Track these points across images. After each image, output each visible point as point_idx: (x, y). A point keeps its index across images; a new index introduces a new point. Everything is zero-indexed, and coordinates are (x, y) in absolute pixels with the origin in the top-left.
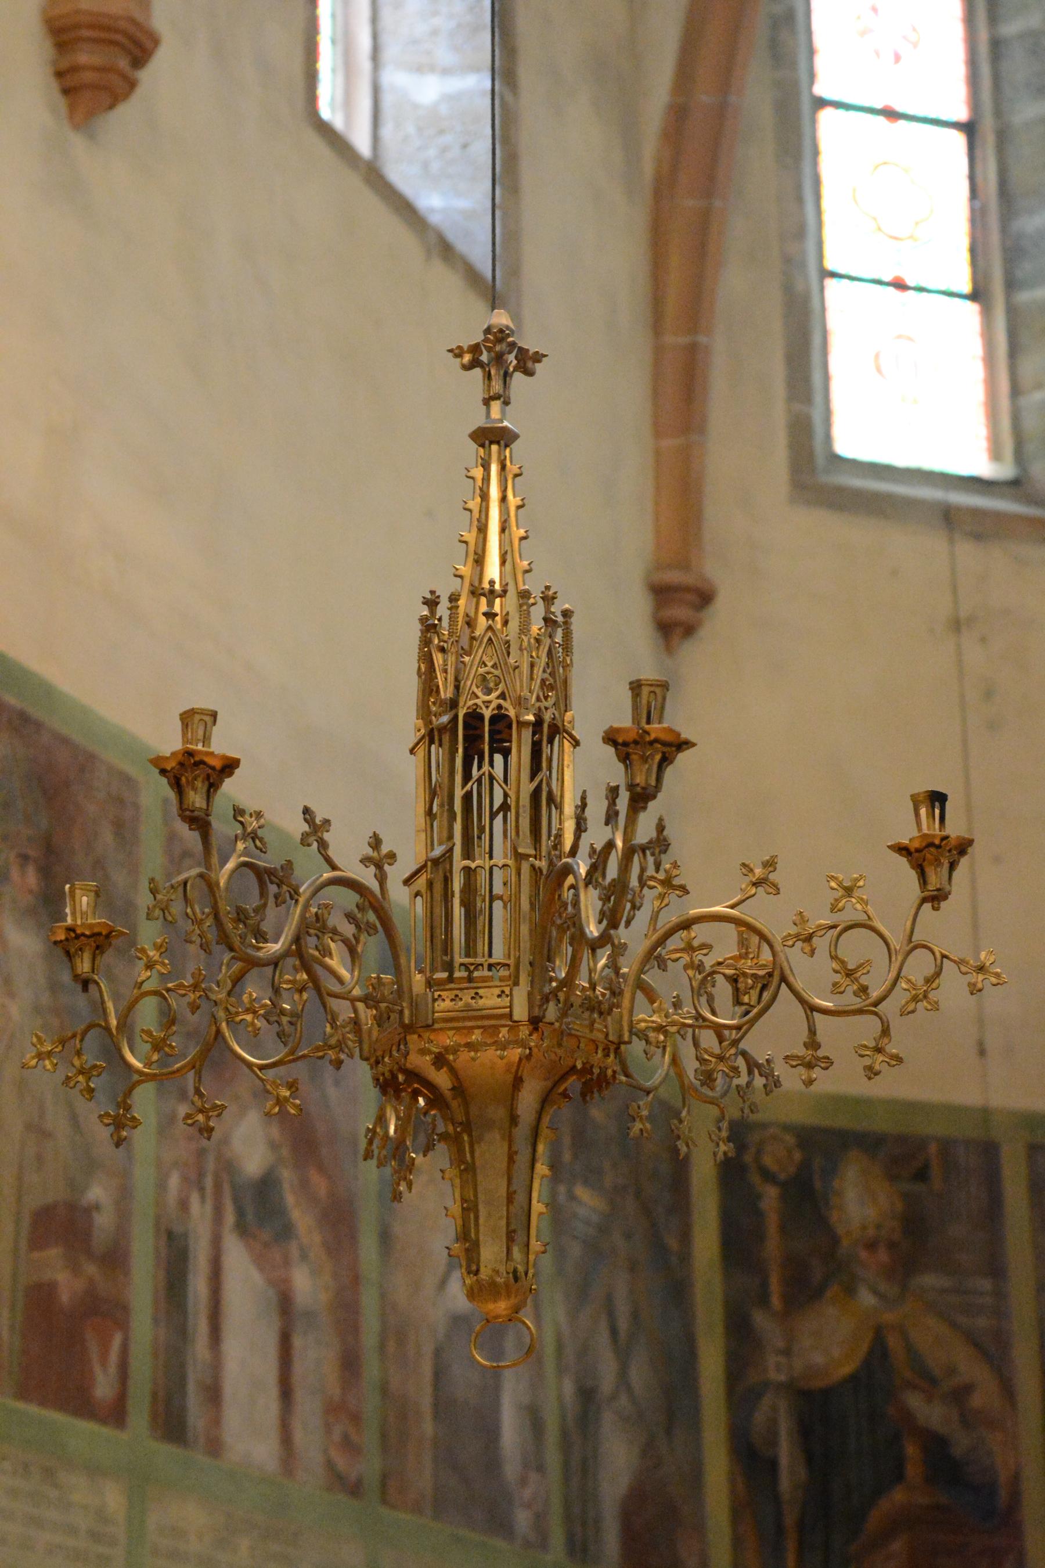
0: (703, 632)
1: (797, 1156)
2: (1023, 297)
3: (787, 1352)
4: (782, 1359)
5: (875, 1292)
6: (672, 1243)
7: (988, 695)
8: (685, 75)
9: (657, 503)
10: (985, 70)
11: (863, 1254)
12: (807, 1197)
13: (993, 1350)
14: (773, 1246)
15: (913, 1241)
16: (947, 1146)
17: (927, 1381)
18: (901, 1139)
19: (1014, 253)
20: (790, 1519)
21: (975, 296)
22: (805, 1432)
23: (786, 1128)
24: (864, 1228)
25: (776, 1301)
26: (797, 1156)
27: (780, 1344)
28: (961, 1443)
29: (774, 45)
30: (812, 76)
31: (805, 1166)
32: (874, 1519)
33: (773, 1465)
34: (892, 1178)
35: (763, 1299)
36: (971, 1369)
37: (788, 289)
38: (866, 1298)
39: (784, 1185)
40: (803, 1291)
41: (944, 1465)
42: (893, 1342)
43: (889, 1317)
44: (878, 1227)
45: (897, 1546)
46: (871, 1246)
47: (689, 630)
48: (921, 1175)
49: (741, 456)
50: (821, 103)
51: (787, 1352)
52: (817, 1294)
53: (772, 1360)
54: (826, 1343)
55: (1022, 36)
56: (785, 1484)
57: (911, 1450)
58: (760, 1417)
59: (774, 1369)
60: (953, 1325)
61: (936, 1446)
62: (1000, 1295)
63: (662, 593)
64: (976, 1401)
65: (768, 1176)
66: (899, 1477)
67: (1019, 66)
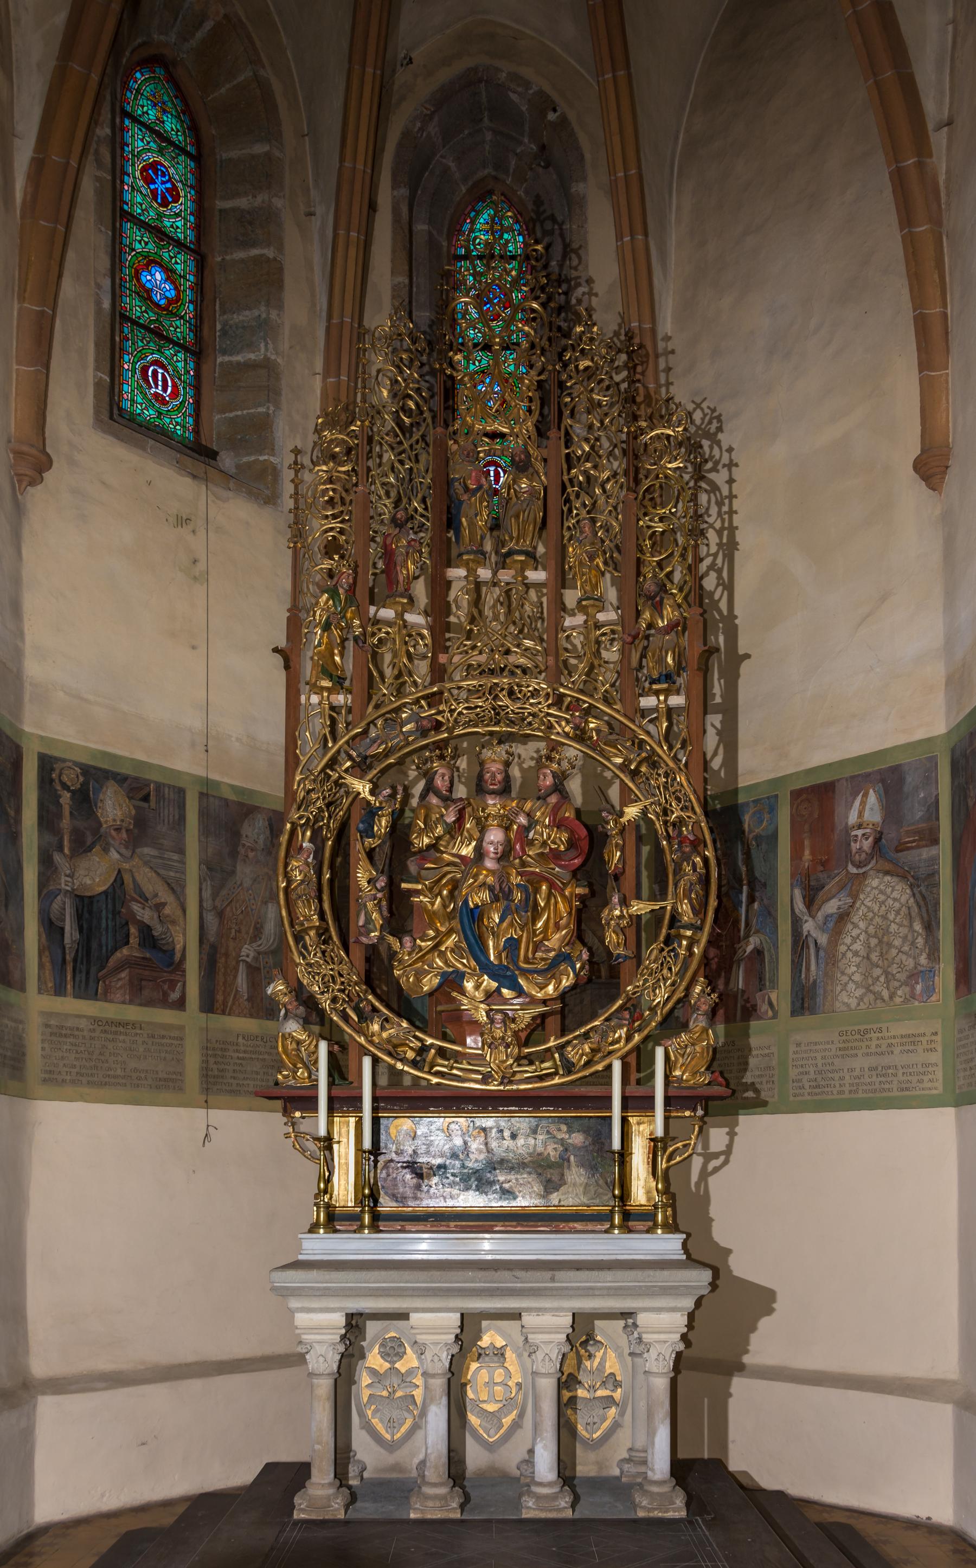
1: (81, 779)
3: (71, 876)
4: (69, 879)
5: (118, 852)
6: (12, 813)
12: (85, 800)
13: (176, 888)
14: (66, 823)
17: (143, 898)
18: (136, 779)
20: (69, 958)
22: (79, 917)
23: (76, 764)
25: (66, 851)
26: (81, 779)
27: (68, 872)
28: (158, 930)
31: (85, 785)
32: (112, 962)
33: (62, 930)
35: (60, 848)
36: (165, 896)
39: (73, 792)
40: (81, 847)
42: (127, 878)
43: (126, 866)
51: (71, 876)
52: (90, 849)
53: (63, 879)
54: (94, 873)
56: (67, 940)
57: (133, 930)
58: (56, 906)
59: (64, 883)
60: (158, 874)
62: (183, 862)
64: (167, 911)
65: (65, 787)
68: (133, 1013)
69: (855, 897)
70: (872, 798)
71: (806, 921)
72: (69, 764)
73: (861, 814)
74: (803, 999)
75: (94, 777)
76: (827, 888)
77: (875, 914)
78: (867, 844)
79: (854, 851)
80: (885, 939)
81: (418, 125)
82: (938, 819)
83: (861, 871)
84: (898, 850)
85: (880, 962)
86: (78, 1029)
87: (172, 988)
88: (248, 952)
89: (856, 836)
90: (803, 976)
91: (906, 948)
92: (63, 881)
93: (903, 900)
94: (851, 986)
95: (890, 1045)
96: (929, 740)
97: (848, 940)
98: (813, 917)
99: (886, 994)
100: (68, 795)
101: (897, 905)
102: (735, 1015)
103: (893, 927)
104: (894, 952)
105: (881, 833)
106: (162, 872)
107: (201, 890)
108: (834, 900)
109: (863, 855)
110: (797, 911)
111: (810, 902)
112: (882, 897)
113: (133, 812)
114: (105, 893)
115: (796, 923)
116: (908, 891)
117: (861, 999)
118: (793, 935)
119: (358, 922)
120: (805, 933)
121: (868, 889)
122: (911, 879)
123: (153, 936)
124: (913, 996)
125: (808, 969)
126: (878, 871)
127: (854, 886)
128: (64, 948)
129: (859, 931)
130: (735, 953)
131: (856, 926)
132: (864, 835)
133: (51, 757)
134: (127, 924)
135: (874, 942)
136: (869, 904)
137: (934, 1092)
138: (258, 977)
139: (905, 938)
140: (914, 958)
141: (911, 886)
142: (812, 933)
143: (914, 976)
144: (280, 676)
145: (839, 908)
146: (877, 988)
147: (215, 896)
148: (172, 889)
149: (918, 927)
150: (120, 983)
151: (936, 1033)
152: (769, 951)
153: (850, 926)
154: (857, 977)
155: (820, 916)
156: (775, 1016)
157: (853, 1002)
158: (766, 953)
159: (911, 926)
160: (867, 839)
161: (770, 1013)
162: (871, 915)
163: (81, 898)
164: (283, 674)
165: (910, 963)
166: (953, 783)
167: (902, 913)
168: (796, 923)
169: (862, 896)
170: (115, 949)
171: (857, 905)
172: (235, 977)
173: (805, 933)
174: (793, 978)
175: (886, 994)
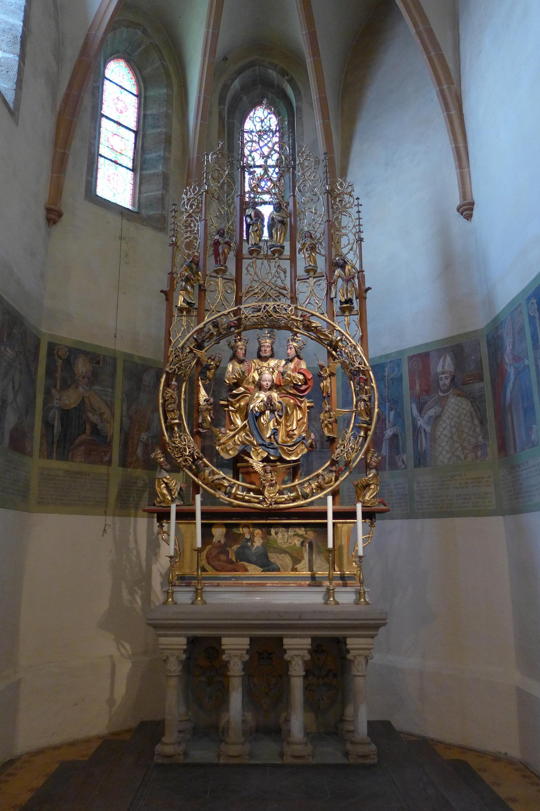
0: (59, 224)
1: (68, 353)
2: (145, 172)
3: (60, 400)
4: (58, 401)
5: (83, 388)
6: (33, 370)
7: (127, 256)
8: (70, 87)
9: (50, 188)
10: (142, 121)
11: (81, 379)
12: (69, 363)
13: (110, 405)
14: (58, 374)
15: (94, 378)
16: (105, 357)
19: (143, 162)
20: (55, 440)
21: (133, 170)
22: (62, 419)
23: (66, 346)
24: (82, 373)
25: (58, 388)
26: (68, 353)
27: (58, 398)
28: (100, 426)
29: (93, 94)
30: (101, 109)
31: (69, 356)
32: (77, 441)
33: (53, 426)
34: (90, 363)
35: (55, 387)
37: (90, 150)
38: (81, 389)
39: (63, 360)
40: (65, 386)
41: (95, 430)
42: (87, 400)
44: (86, 373)
45: (82, 448)
46: (84, 377)
47: (55, 222)
48: (98, 363)
49: (73, 185)
50: (103, 116)
51: (60, 400)
52: (69, 387)
53: (56, 401)
54: (70, 399)
55: (151, 115)
57: (88, 426)
58: (51, 414)
60: (102, 398)
61: (94, 427)
63: (49, 210)
64: (105, 416)
65: (60, 357)
66: (84, 432)
67: (150, 121)
68: (86, 467)
69: (443, 407)
70: (448, 359)
71: (419, 420)
72: (62, 346)
73: (443, 367)
74: (420, 459)
75: (75, 352)
76: (429, 403)
77: (454, 416)
78: (447, 382)
79: (441, 385)
80: (460, 428)
81: (230, 82)
82: (482, 369)
83: (446, 394)
84: (463, 384)
85: (458, 440)
86: (57, 476)
87: (106, 455)
88: (144, 436)
89: (442, 378)
90: (419, 447)
91: (471, 433)
92: (55, 402)
93: (468, 408)
94: (444, 452)
95: (466, 483)
96: (475, 331)
97: (441, 429)
98: (423, 418)
99: (462, 457)
100: (61, 361)
101: (465, 412)
102: (385, 467)
103: (464, 423)
104: (465, 435)
105: (454, 376)
106: (104, 398)
107: (122, 406)
108: (432, 409)
109: (446, 387)
110: (414, 415)
111: (420, 411)
112: (457, 408)
113: (92, 369)
114: (75, 408)
115: (414, 420)
116: (470, 404)
117: (449, 459)
118: (413, 427)
119: (198, 420)
120: (419, 426)
121: (450, 404)
122: (471, 399)
123: (97, 429)
124: (476, 457)
125: (421, 444)
126: (454, 395)
127: (442, 402)
128: (53, 435)
129: (446, 425)
130: (384, 436)
131: (444, 422)
132: (445, 377)
133: (54, 344)
134: (85, 423)
135: (454, 430)
136: (451, 411)
137: (491, 508)
138: (148, 449)
139: (470, 428)
140: (476, 438)
141: (471, 402)
142: (422, 426)
143: (476, 447)
144: (163, 305)
145: (435, 413)
146: (458, 453)
147: (129, 408)
148: (108, 406)
149: (476, 422)
150: (80, 453)
151: (490, 477)
152: (401, 434)
153: (441, 422)
154: (447, 448)
155: (426, 417)
156: (406, 468)
157: (446, 461)
158: (399, 436)
159: (473, 422)
160: (447, 379)
161: (403, 466)
162: (452, 416)
163: (63, 410)
164: (165, 303)
165: (473, 440)
166: (488, 351)
167: (468, 415)
168: (414, 420)
169: (446, 407)
170: (79, 435)
171: (445, 411)
172: (137, 449)
173: (419, 426)
174: (414, 448)
175: (462, 457)
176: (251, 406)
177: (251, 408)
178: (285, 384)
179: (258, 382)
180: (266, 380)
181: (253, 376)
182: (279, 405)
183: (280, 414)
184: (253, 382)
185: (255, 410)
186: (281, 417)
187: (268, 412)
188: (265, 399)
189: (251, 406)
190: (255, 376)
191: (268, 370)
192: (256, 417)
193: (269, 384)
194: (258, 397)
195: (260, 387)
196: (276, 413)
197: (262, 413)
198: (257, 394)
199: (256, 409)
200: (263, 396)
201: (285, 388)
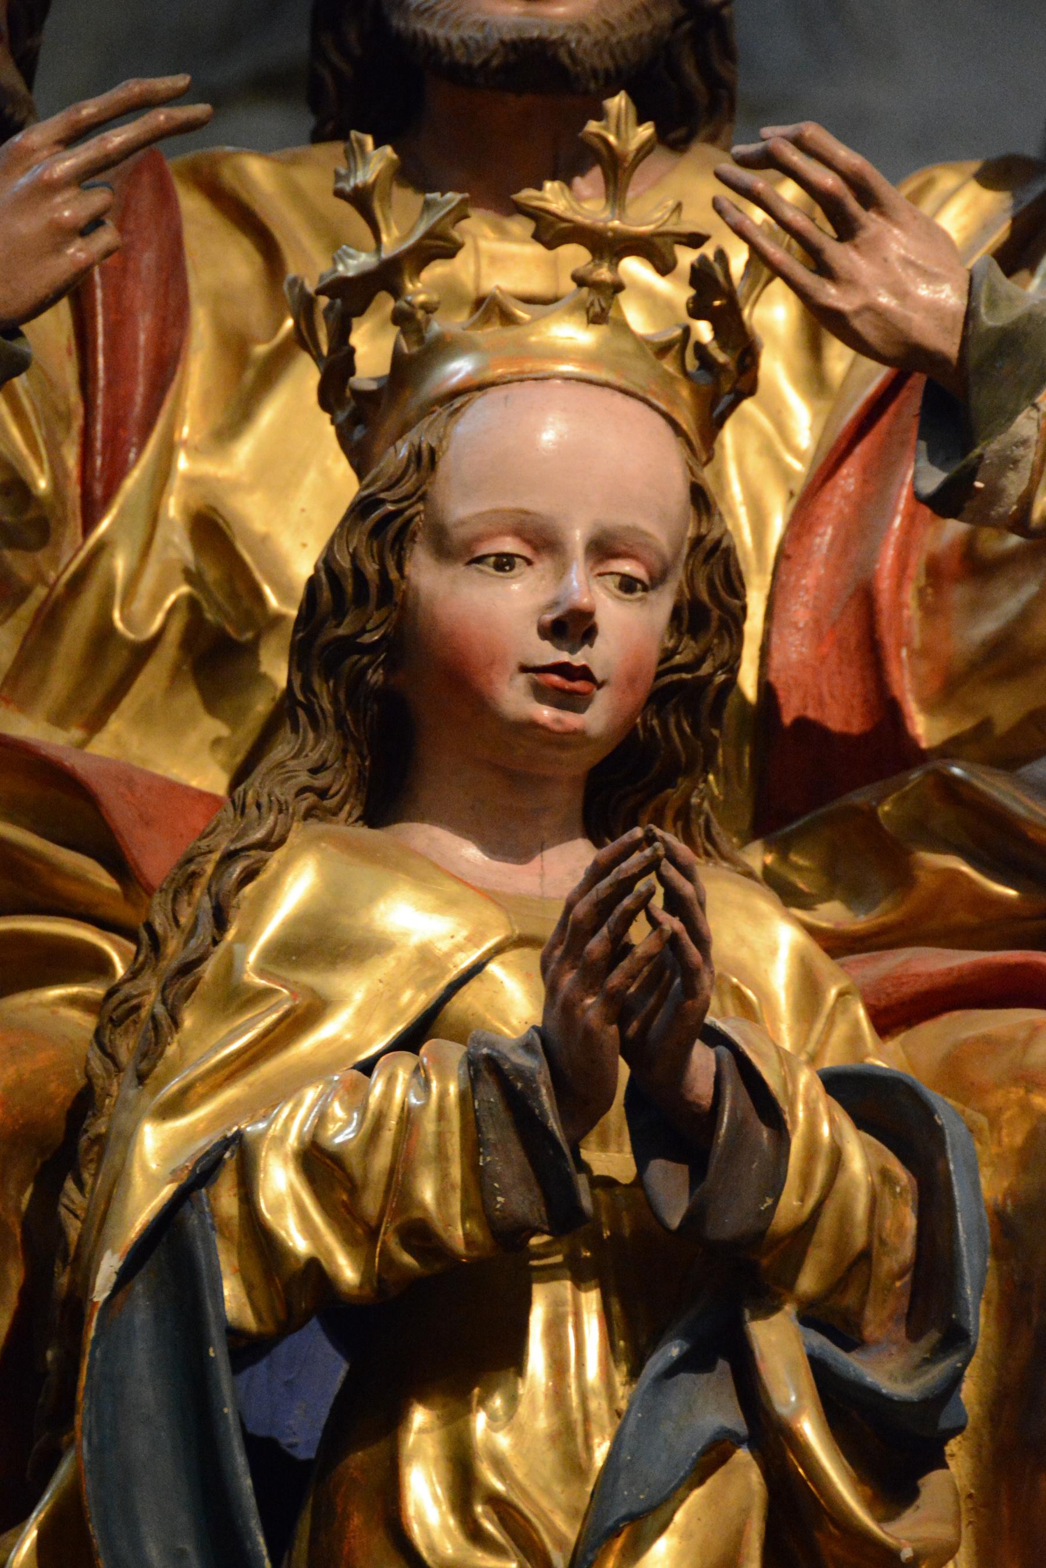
176: (156, 1150)
177: (143, 1203)
178: (1005, 708)
179: (334, 589)
180: (544, 542)
181: (210, 529)
182: (860, 1156)
183: (888, 1372)
184: (213, 653)
185: (260, 1240)
186: (893, 1446)
187: (568, 1333)
188: (513, 1001)
189: (156, 1150)
190: (253, 513)
191: (600, 301)
192: (263, 1451)
193: (628, 631)
194: (323, 944)
195: (375, 705)
196: (778, 1343)
197: (436, 1328)
198: (297, 886)
199: (279, 1181)
200: (432, 932)
201: (999, 789)
